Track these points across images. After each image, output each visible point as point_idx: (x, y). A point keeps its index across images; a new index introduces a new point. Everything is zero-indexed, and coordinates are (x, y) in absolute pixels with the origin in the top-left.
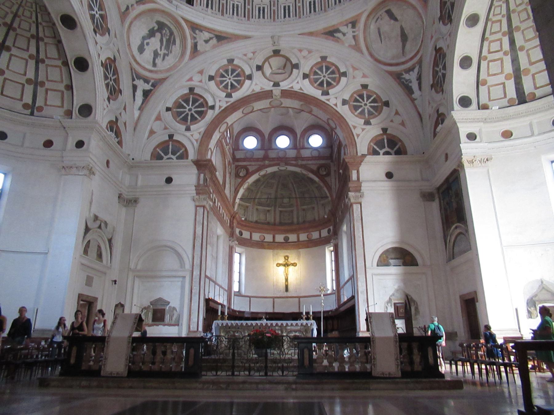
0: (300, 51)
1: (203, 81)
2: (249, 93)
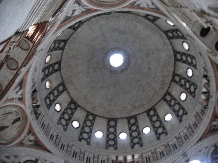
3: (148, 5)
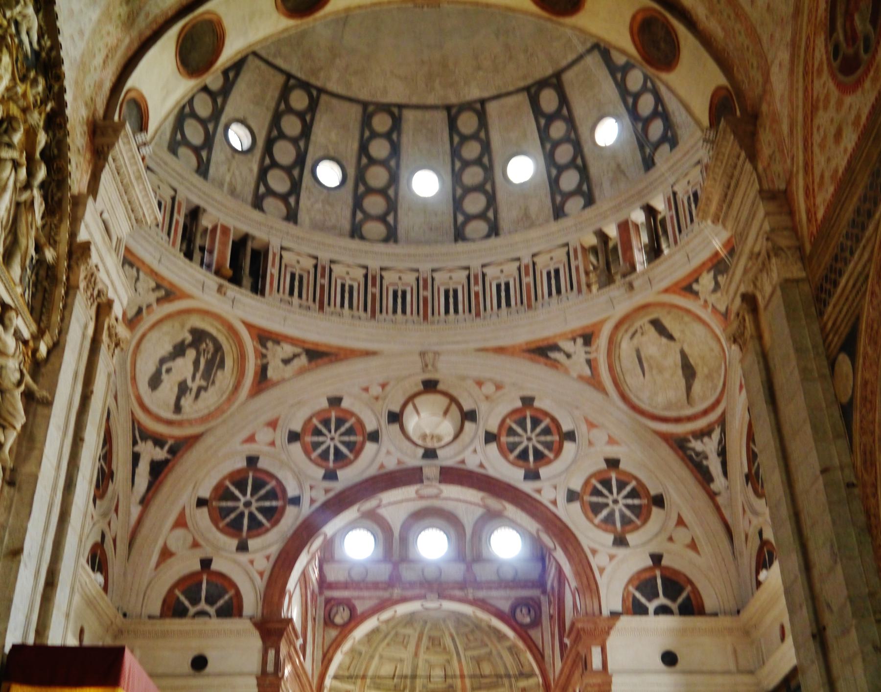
0: (480, 383)
1: (278, 443)
2: (372, 471)
3: (137, 279)
